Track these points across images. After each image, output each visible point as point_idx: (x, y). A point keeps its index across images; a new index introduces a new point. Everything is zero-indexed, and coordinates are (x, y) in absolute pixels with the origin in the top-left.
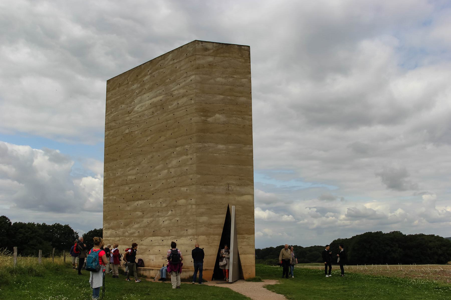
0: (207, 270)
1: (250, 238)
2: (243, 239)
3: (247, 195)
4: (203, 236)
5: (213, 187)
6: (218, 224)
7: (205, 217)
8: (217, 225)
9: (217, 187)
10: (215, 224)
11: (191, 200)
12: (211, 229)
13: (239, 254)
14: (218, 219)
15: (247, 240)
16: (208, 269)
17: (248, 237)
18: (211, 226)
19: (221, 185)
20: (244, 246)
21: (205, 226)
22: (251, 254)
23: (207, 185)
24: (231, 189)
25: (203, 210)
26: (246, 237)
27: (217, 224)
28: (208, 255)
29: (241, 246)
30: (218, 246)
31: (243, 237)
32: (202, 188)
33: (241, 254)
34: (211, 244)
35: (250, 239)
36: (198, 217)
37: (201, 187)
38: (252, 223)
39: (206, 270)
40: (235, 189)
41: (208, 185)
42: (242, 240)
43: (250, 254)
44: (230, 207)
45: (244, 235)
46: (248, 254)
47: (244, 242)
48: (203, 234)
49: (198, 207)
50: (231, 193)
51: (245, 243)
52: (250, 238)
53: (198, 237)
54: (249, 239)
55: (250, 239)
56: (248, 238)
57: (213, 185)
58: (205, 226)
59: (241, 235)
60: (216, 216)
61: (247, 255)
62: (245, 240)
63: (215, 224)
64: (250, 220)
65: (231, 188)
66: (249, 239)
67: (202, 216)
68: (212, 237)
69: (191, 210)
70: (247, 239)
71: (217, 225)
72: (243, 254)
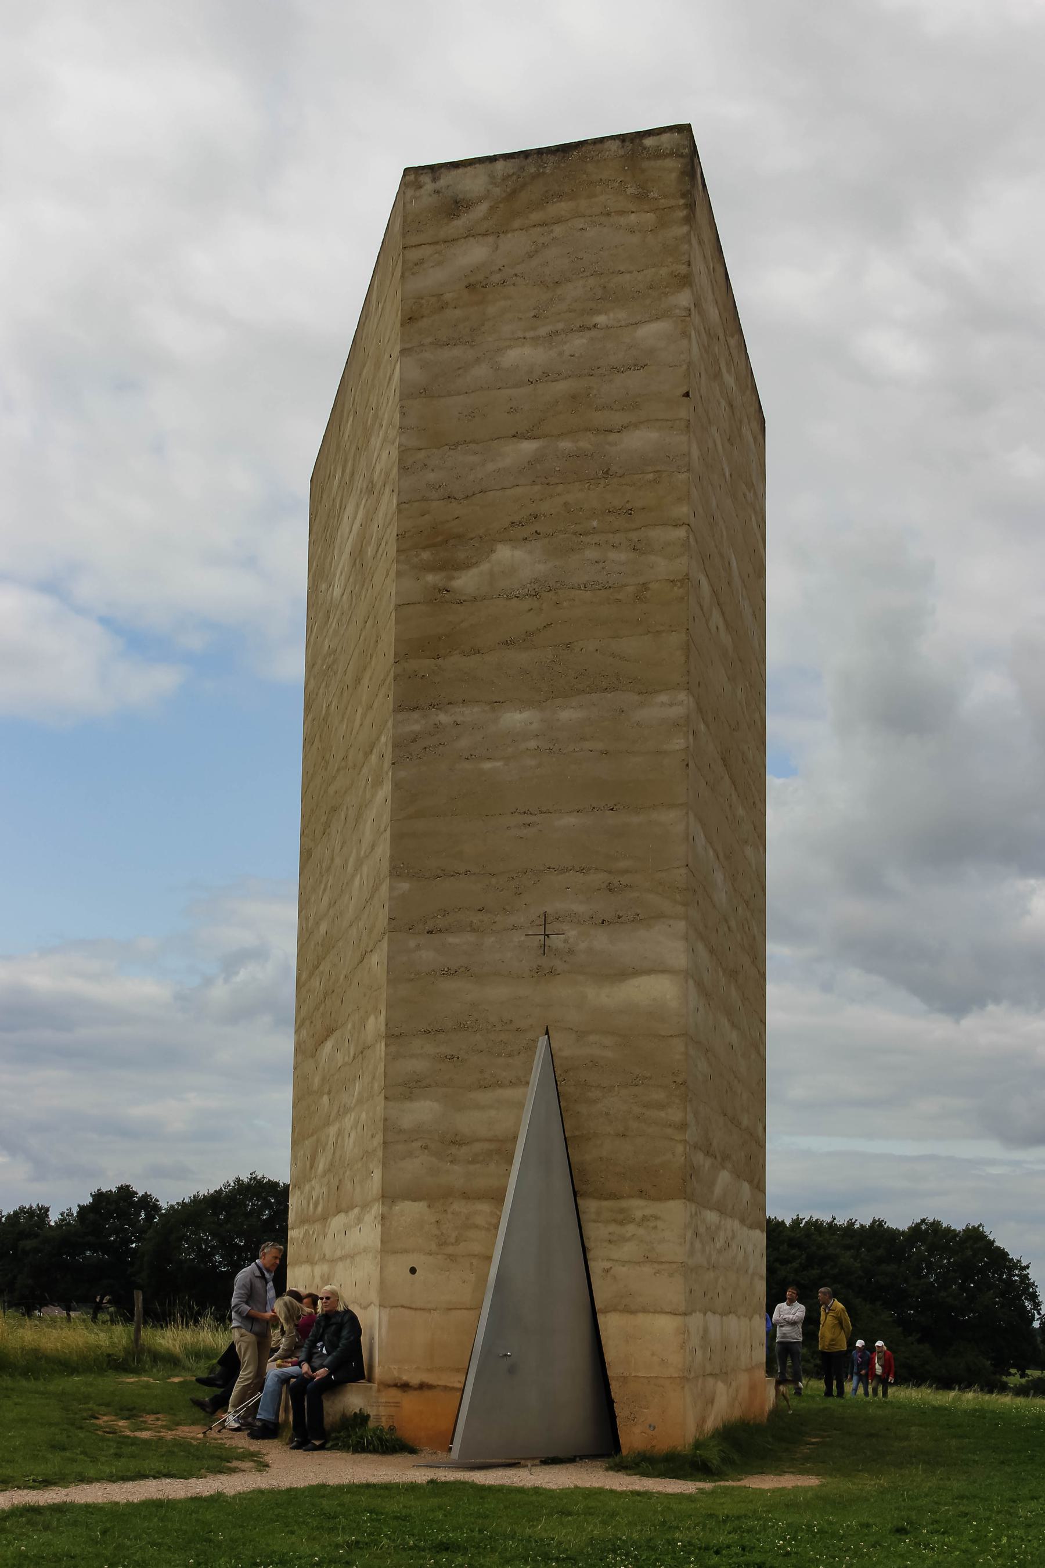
0: (430, 1387)
2: (622, 1223)
4: (416, 1204)
5: (471, 938)
7: (428, 1103)
8: (487, 1146)
9: (493, 939)
10: (478, 1140)
12: (456, 1167)
13: (598, 1305)
15: (641, 1231)
16: (435, 1383)
17: (648, 1212)
18: (454, 1150)
20: (624, 1263)
21: (426, 1147)
22: (662, 1312)
25: (418, 1065)
26: (638, 1214)
29: (607, 1265)
31: (622, 1211)
33: (605, 1312)
34: (450, 1250)
37: (412, 944)
38: (669, 1131)
40: (583, 946)
41: (447, 930)
42: (613, 1228)
43: (655, 1312)
45: (624, 1204)
46: (644, 1310)
47: (624, 1239)
48: (414, 1196)
51: (628, 1250)
55: (655, 1227)
56: (645, 1218)
57: (474, 930)
58: (426, 1147)
59: (606, 1199)
61: (641, 1318)
62: (630, 1229)
63: (478, 1140)
64: (663, 1114)
65: (566, 941)
70: (639, 1225)
72: (615, 1310)
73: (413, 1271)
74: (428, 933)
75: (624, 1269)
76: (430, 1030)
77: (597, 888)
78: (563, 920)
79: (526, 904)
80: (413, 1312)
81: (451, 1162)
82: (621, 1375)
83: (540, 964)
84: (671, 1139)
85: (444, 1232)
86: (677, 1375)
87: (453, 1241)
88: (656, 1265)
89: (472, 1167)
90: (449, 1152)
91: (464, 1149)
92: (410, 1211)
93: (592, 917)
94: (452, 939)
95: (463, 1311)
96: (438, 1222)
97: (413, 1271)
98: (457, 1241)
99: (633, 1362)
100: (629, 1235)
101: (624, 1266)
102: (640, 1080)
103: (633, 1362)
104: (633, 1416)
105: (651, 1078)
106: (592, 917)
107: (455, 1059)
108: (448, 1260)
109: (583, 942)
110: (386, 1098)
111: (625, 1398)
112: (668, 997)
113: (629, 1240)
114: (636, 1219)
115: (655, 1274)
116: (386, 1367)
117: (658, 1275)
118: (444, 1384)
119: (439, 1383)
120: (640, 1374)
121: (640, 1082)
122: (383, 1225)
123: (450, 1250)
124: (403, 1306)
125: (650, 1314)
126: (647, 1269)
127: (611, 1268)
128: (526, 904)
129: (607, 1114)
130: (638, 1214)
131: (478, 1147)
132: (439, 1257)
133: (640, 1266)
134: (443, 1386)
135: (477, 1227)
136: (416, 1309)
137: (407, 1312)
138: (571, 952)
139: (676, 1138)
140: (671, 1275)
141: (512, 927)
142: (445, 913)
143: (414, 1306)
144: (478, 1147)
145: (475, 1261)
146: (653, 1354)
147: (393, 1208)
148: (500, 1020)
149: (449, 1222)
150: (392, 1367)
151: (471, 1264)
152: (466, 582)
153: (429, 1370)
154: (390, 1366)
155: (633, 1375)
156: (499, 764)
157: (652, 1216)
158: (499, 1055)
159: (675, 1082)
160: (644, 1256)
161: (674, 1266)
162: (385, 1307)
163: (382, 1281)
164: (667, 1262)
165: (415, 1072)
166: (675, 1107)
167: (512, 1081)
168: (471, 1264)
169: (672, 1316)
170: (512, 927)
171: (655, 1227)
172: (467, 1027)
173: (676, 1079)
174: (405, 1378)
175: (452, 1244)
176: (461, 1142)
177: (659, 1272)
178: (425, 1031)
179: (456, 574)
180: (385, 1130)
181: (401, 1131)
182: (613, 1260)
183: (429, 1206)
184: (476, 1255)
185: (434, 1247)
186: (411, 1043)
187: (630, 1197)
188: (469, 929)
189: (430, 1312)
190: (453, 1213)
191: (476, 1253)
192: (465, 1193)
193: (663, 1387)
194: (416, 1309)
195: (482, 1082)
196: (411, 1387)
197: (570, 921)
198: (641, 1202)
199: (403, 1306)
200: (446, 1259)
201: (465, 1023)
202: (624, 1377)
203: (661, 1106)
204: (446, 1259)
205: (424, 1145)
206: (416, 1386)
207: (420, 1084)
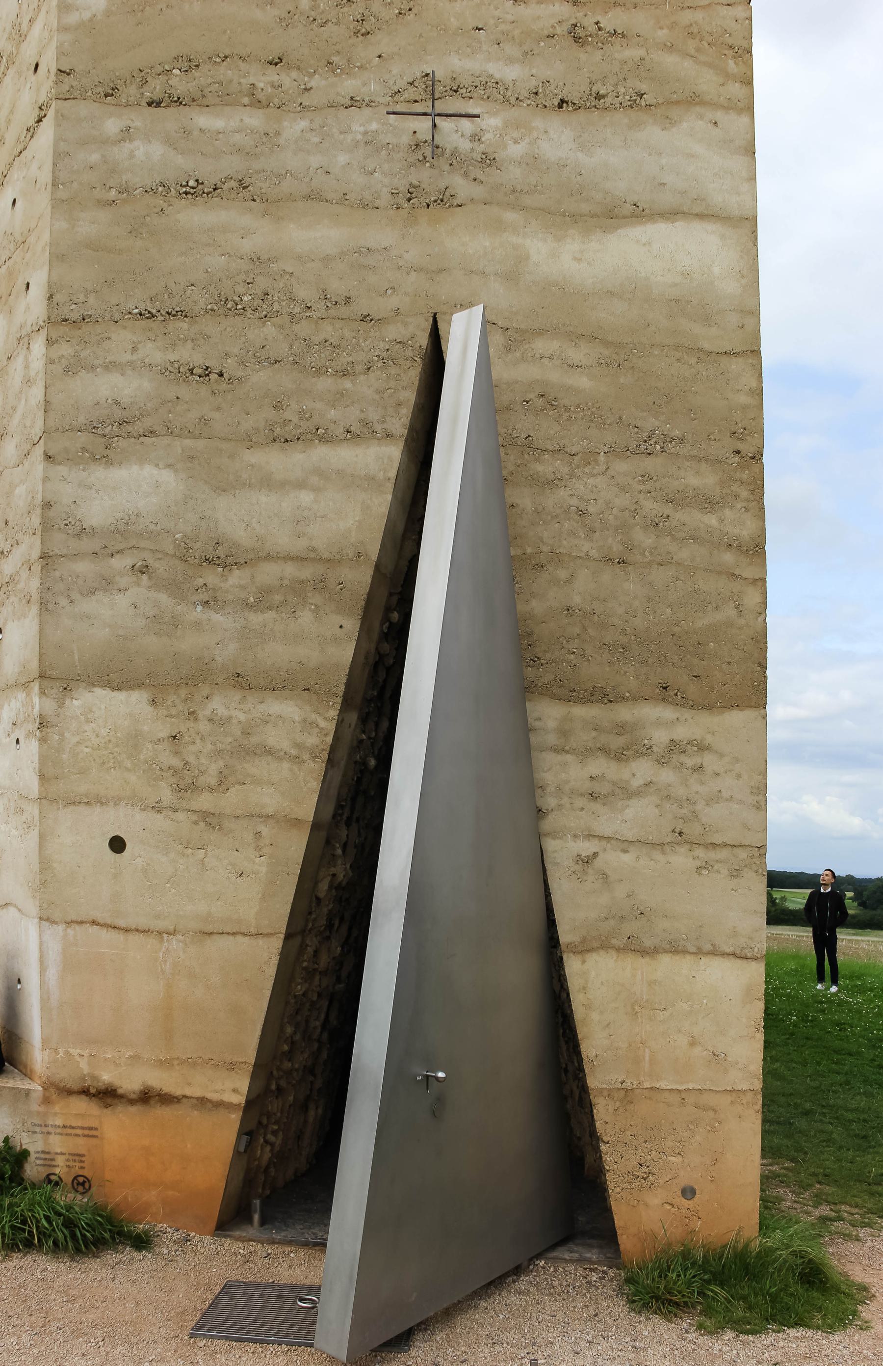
0: (167, 1099)
1: (703, 748)
2: (620, 756)
3: (672, 214)
4: (122, 696)
5: (254, 119)
6: (300, 559)
7: (148, 471)
8: (290, 570)
9: (303, 124)
10: (269, 558)
12: (217, 618)
13: (565, 936)
14: (306, 497)
15: (666, 776)
16: (178, 1092)
17: (681, 733)
18: (211, 576)
19: (353, 102)
20: (625, 845)
21: (144, 570)
22: (715, 952)
23: (179, 102)
24: (465, 145)
26: (660, 738)
27: (289, 558)
28: (173, 933)
29: (586, 848)
30: (296, 823)
31: (621, 729)
32: (127, 133)
33: (583, 949)
34: (204, 801)
35: (708, 760)
36: (62, 470)
37: (112, 126)
38: (728, 557)
39: (232, 1067)
40: (515, 150)
41: (198, 101)
42: (598, 766)
43: (699, 952)
44: (441, 326)
45: (624, 713)
46: (676, 949)
47: (628, 793)
49: (65, 350)
50: (461, 187)
52: (703, 748)
53: (61, 704)
54: (690, 762)
55: (700, 768)
56: (674, 746)
57: (257, 103)
58: (144, 570)
59: (583, 701)
61: (666, 962)
63: (269, 558)
64: (712, 520)
65: (475, 138)
66: (690, 762)
67: (107, 460)
68: (222, 711)
70: (661, 762)
71: (290, 570)
72: (605, 946)
73: (117, 845)
74: (150, 104)
75: (627, 858)
76: (154, 311)
77: (546, 33)
78: (468, 95)
79: (380, 56)
80: (119, 937)
82: (619, 1086)
83: (415, 182)
84: (733, 575)
85: (191, 759)
86: (745, 1087)
87: (213, 781)
88: (700, 852)
89: (256, 619)
90: (200, 581)
91: (237, 577)
93: (536, 93)
94: (203, 120)
95: (240, 938)
96: (175, 737)
97: (117, 845)
98: (222, 784)
99: (647, 1058)
100: (636, 783)
101: (625, 851)
102: (656, 443)
103: (647, 1058)
104: (644, 1169)
105: (682, 440)
106: (536, 93)
107: (214, 377)
108: (202, 824)
109: (516, 142)
110: (48, 457)
111: (629, 1133)
112: (716, 270)
113: (638, 793)
114: (655, 749)
115: (698, 869)
116: (61, 1051)
117: (705, 872)
118: (198, 1094)
119: (188, 1092)
120: (663, 1085)
121: (658, 447)
122: (43, 740)
123: (204, 801)
124: (94, 923)
125: (688, 957)
127: (595, 854)
128: (380, 56)
129: (581, 513)
130: (660, 738)
131: (269, 573)
132: (181, 816)
133: (664, 853)
134: (198, 1099)
135: (269, 752)
136: (127, 930)
137: (105, 935)
138: (488, 161)
139: (745, 575)
140: (735, 874)
141: (348, 102)
142: (190, 65)
143: (122, 923)
144: (269, 573)
145: (265, 830)
146: (693, 1043)
147: (68, 702)
148: (322, 297)
149: (202, 739)
150: (75, 1052)
151: (258, 835)
153: (165, 1064)
154: (71, 1051)
155: (647, 1085)
157: (689, 743)
158: (320, 371)
159: (738, 452)
160: (673, 831)
161: (743, 854)
162: (54, 922)
163: (45, 864)
164: (726, 845)
165: (116, 403)
166: (739, 506)
167: (352, 429)
168: (258, 835)
169: (739, 961)
170: (348, 102)
171: (700, 768)
172: (244, 309)
173: (740, 446)
174: (107, 1077)
175: (211, 790)
176: (230, 560)
177: (707, 866)
178: (141, 315)
180: (47, 526)
181: (82, 532)
182: (600, 838)
184: (267, 816)
185: (167, 795)
186: (109, 338)
187: (638, 698)
188: (246, 100)
189: (162, 938)
191: (270, 811)
192: (239, 675)
193: (715, 1111)
194: (127, 930)
195: (278, 430)
196: (122, 1097)
197: (485, 97)
198: (667, 713)
199: (94, 923)
200: (196, 823)
201: (237, 299)
202: (627, 1090)
203: (710, 504)
204: (196, 823)
205: (140, 563)
206: (133, 1096)
207: (130, 428)
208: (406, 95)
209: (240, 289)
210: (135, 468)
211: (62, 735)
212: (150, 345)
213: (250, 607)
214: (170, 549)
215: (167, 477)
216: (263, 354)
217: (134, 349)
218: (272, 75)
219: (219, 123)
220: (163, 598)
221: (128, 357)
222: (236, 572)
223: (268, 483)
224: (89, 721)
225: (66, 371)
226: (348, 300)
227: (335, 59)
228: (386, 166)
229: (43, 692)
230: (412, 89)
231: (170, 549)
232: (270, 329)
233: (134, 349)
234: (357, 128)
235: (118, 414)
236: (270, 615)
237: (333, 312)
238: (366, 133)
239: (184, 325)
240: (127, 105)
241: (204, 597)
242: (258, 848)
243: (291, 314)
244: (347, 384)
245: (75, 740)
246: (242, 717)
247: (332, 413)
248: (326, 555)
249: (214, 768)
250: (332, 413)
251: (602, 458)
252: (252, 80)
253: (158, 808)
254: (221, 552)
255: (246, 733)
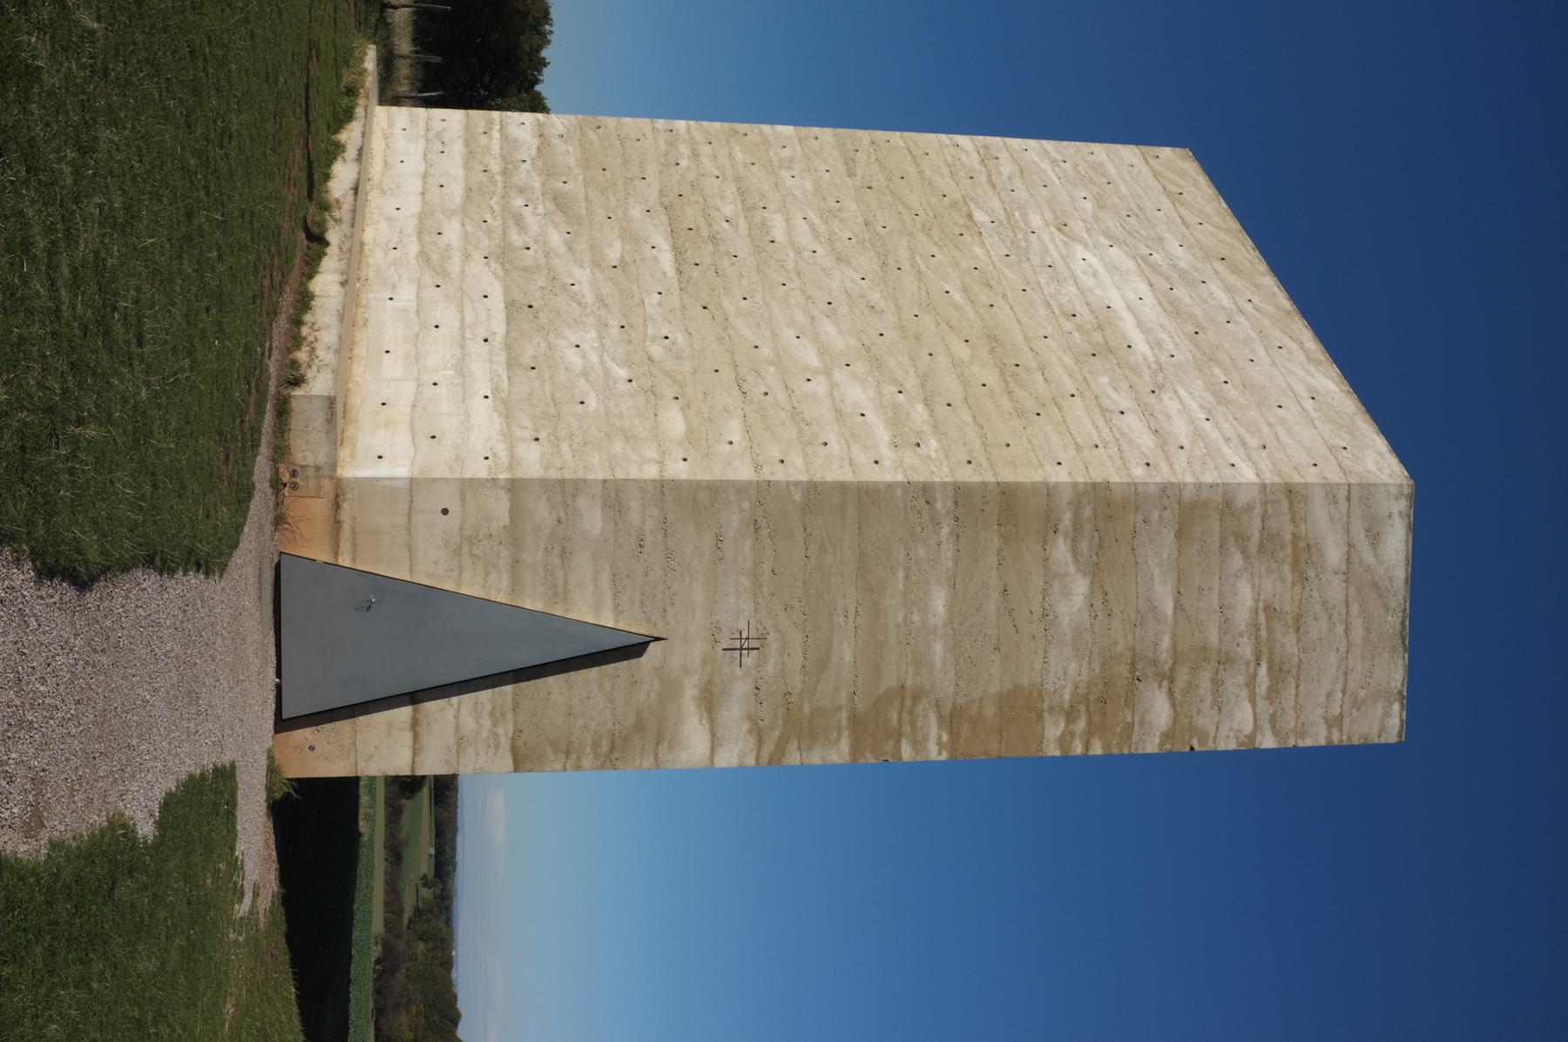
2: (492, 714)
3: (713, 734)
4: (507, 514)
5: (749, 564)
8: (561, 583)
9: (747, 585)
11: (685, 460)
12: (541, 553)
14: (591, 588)
15: (485, 734)
18: (557, 550)
20: (456, 717)
25: (634, 516)
27: (566, 582)
31: (503, 715)
32: (742, 510)
34: (465, 549)
45: (509, 716)
47: (478, 717)
48: (516, 511)
51: (468, 722)
52: (497, 747)
53: (502, 488)
60: (605, 578)
62: (487, 723)
63: (565, 574)
67: (604, 506)
69: (635, 458)
71: (561, 583)
73: (445, 512)
75: (451, 718)
81: (546, 549)
85: (482, 543)
88: (455, 748)
89: (541, 569)
91: (557, 561)
92: (501, 508)
97: (445, 512)
98: (472, 555)
113: (477, 722)
126: (452, 739)
129: (588, 698)
131: (560, 575)
132: (459, 539)
136: (409, 515)
152: (1061, 550)
156: (901, 587)
157: (499, 742)
158: (643, 593)
168: (453, 570)
179: (1069, 542)
183: (505, 527)
185: (467, 533)
188: (757, 561)
190: (499, 550)
194: (409, 515)
195: (618, 576)
208: (759, 626)
209: (676, 560)
210: (601, 518)
211: (490, 488)
212: (653, 523)
213: (546, 566)
214: (568, 533)
215: (598, 531)
216: (649, 569)
217: (650, 516)
218: (768, 571)
219: (747, 550)
220: (548, 531)
221: (647, 514)
222: (559, 561)
223: (596, 573)
224: (496, 500)
225: (642, 488)
226: (673, 604)
227: (775, 597)
228: (729, 618)
229: (507, 480)
230: (762, 628)
231: (568, 533)
232: (660, 573)
233: (650, 516)
234: (745, 607)
235: (623, 510)
236: (542, 575)
237: (667, 598)
238: (743, 610)
239: (661, 537)
240: (755, 511)
241: (549, 548)
242: (447, 571)
243: (666, 581)
244: (638, 604)
245: (488, 493)
246: (501, 564)
247: (625, 599)
248: (568, 597)
249: (479, 552)
250: (625, 599)
251: (611, 706)
252: (766, 562)
253: (462, 529)
254: (568, 554)
255: (494, 565)
